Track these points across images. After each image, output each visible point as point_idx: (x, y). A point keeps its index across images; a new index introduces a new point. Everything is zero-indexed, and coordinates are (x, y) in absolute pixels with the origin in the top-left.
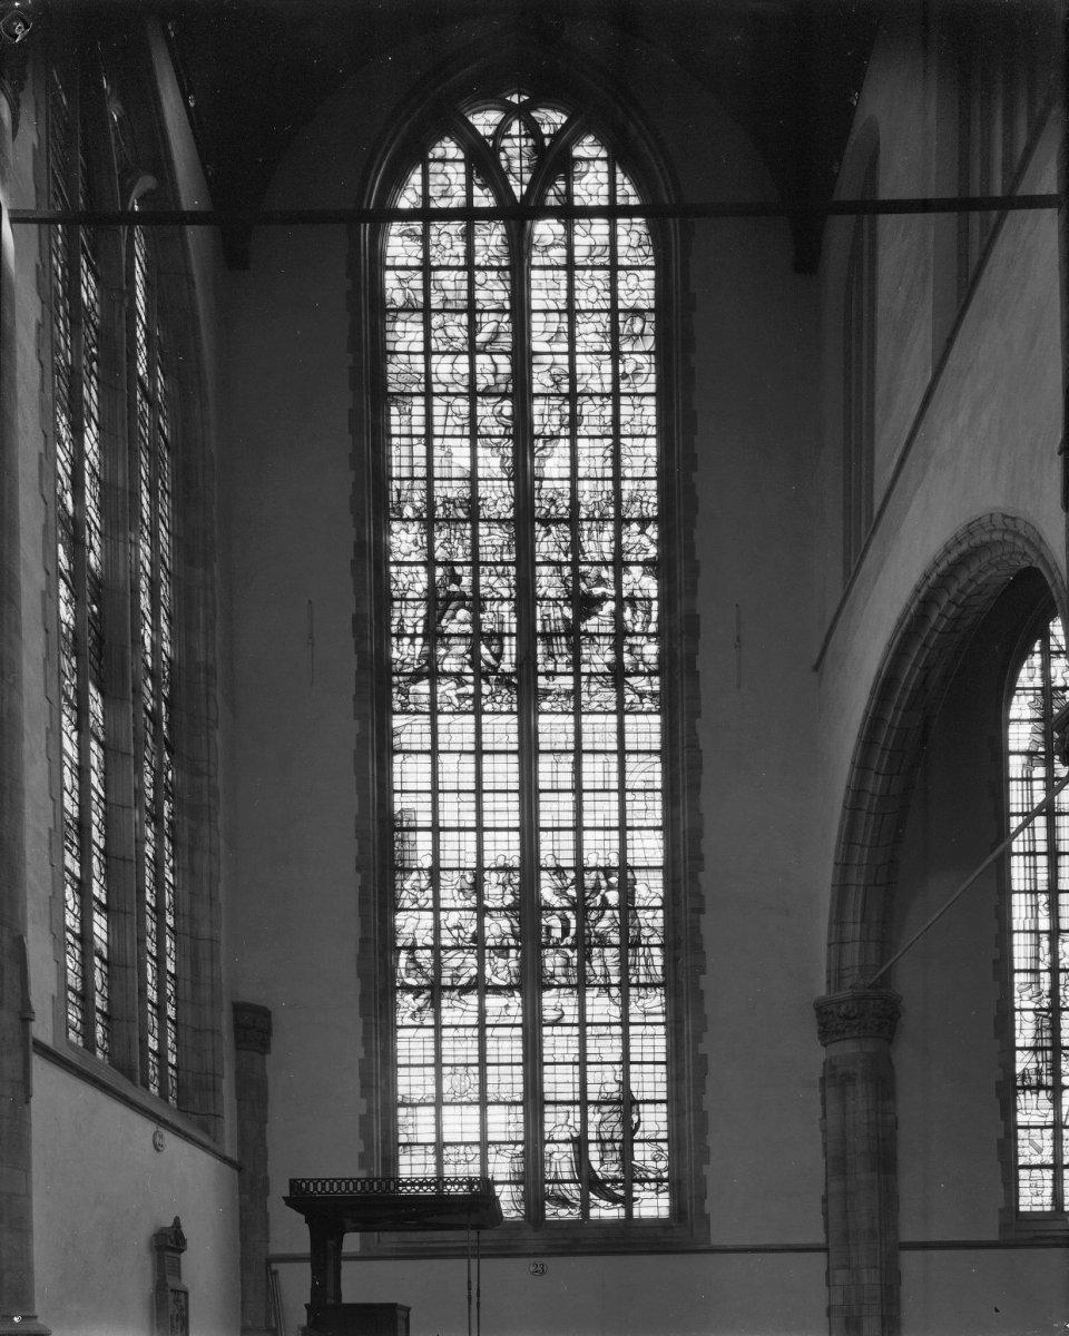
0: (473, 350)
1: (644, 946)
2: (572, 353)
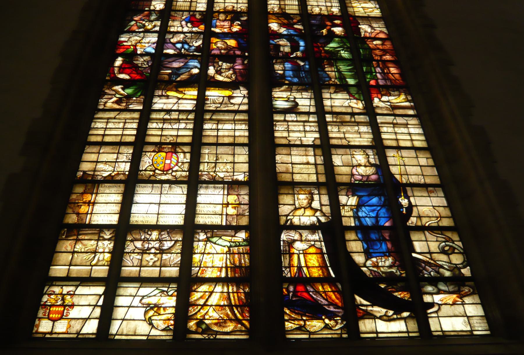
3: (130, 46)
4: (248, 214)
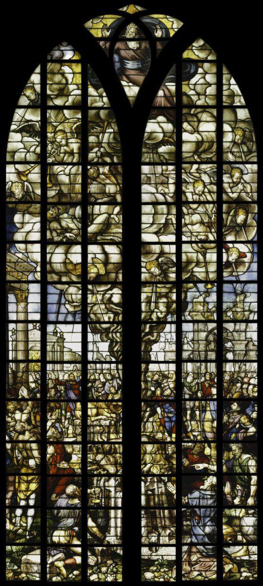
0: (85, 241)
2: (179, 243)
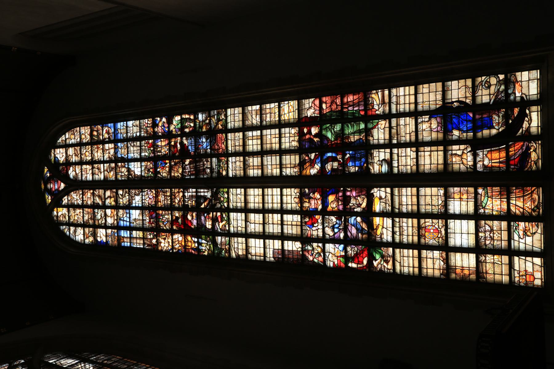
1: (342, 108)
3: (337, 260)
4: (466, 188)
